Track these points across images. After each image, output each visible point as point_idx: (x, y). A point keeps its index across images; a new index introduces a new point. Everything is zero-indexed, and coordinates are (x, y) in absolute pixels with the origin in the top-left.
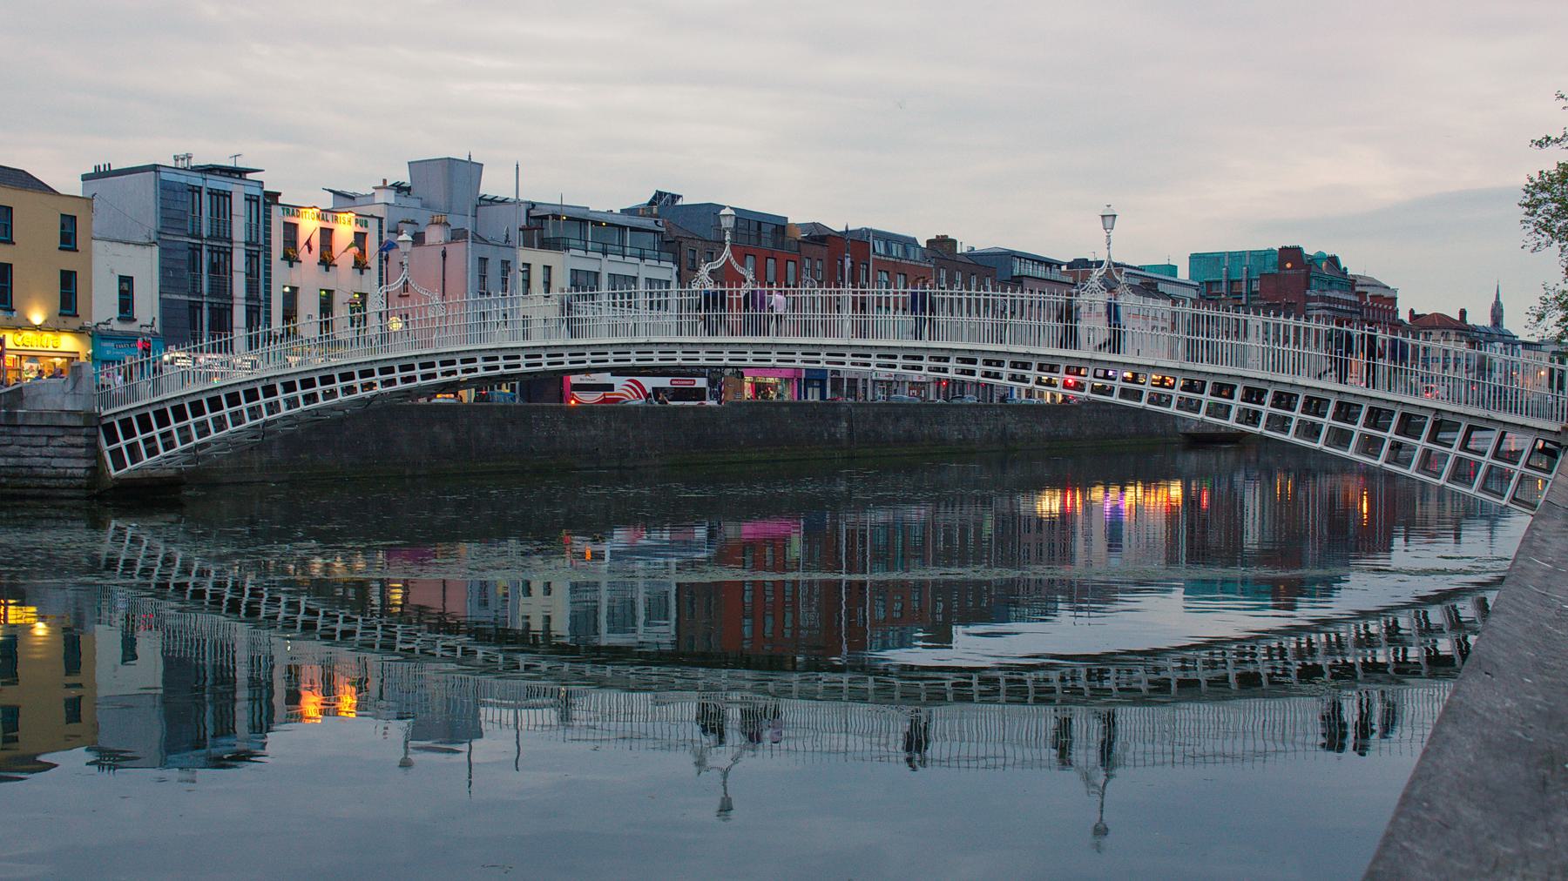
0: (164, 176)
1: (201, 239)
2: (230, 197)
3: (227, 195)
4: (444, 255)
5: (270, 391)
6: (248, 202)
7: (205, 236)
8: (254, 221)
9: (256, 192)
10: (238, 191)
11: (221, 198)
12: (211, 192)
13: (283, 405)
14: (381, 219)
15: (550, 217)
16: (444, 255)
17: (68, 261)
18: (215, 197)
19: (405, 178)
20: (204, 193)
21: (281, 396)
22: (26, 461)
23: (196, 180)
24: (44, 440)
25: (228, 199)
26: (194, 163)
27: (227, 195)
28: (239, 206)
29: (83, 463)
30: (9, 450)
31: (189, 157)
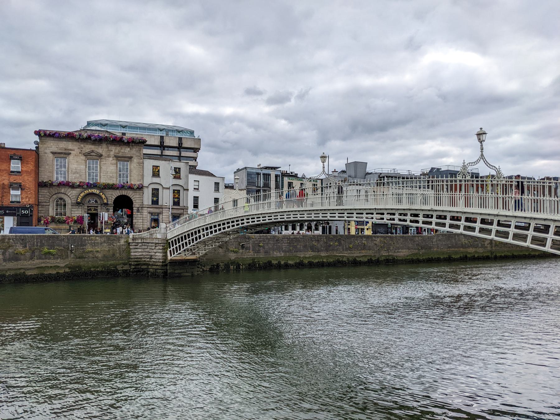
0: (249, 170)
1: (260, 187)
3: (270, 175)
5: (199, 231)
7: (261, 186)
9: (279, 173)
10: (273, 173)
12: (264, 174)
13: (202, 236)
17: (217, 195)
19: (344, 169)
20: (261, 175)
21: (201, 233)
22: (150, 254)
23: (259, 171)
24: (154, 247)
26: (261, 166)
27: (270, 175)
28: (273, 178)
29: (161, 255)
30: (146, 250)
31: (260, 165)
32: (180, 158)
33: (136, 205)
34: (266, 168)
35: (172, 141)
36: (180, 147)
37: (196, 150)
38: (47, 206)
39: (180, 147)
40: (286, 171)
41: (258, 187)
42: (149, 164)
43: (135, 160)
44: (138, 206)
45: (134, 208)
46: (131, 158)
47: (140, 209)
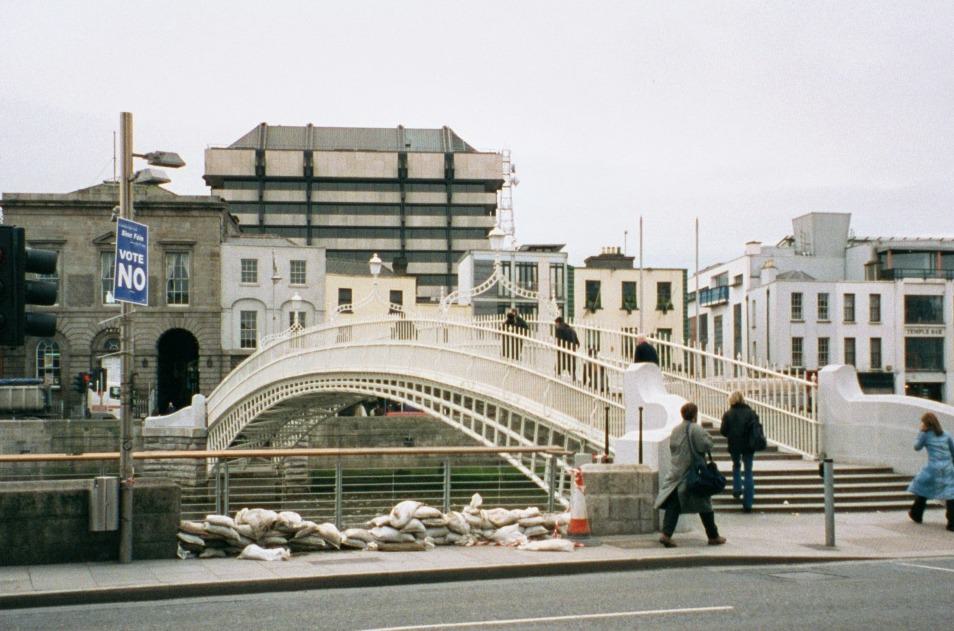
1: (509, 297)
2: (537, 266)
4: (768, 292)
6: (553, 270)
8: (560, 282)
10: (544, 261)
11: (529, 269)
12: (520, 265)
14: (685, 271)
15: (889, 254)
16: (768, 292)
18: (523, 269)
20: (513, 266)
25: (534, 269)
32: (310, 232)
33: (205, 346)
34: (532, 249)
35: (425, 166)
36: (449, 181)
37: (493, 186)
38: (21, 359)
39: (449, 181)
40: (619, 249)
41: (504, 296)
42: (233, 254)
43: (203, 248)
44: (209, 353)
45: (201, 359)
46: (191, 245)
47: (214, 359)
